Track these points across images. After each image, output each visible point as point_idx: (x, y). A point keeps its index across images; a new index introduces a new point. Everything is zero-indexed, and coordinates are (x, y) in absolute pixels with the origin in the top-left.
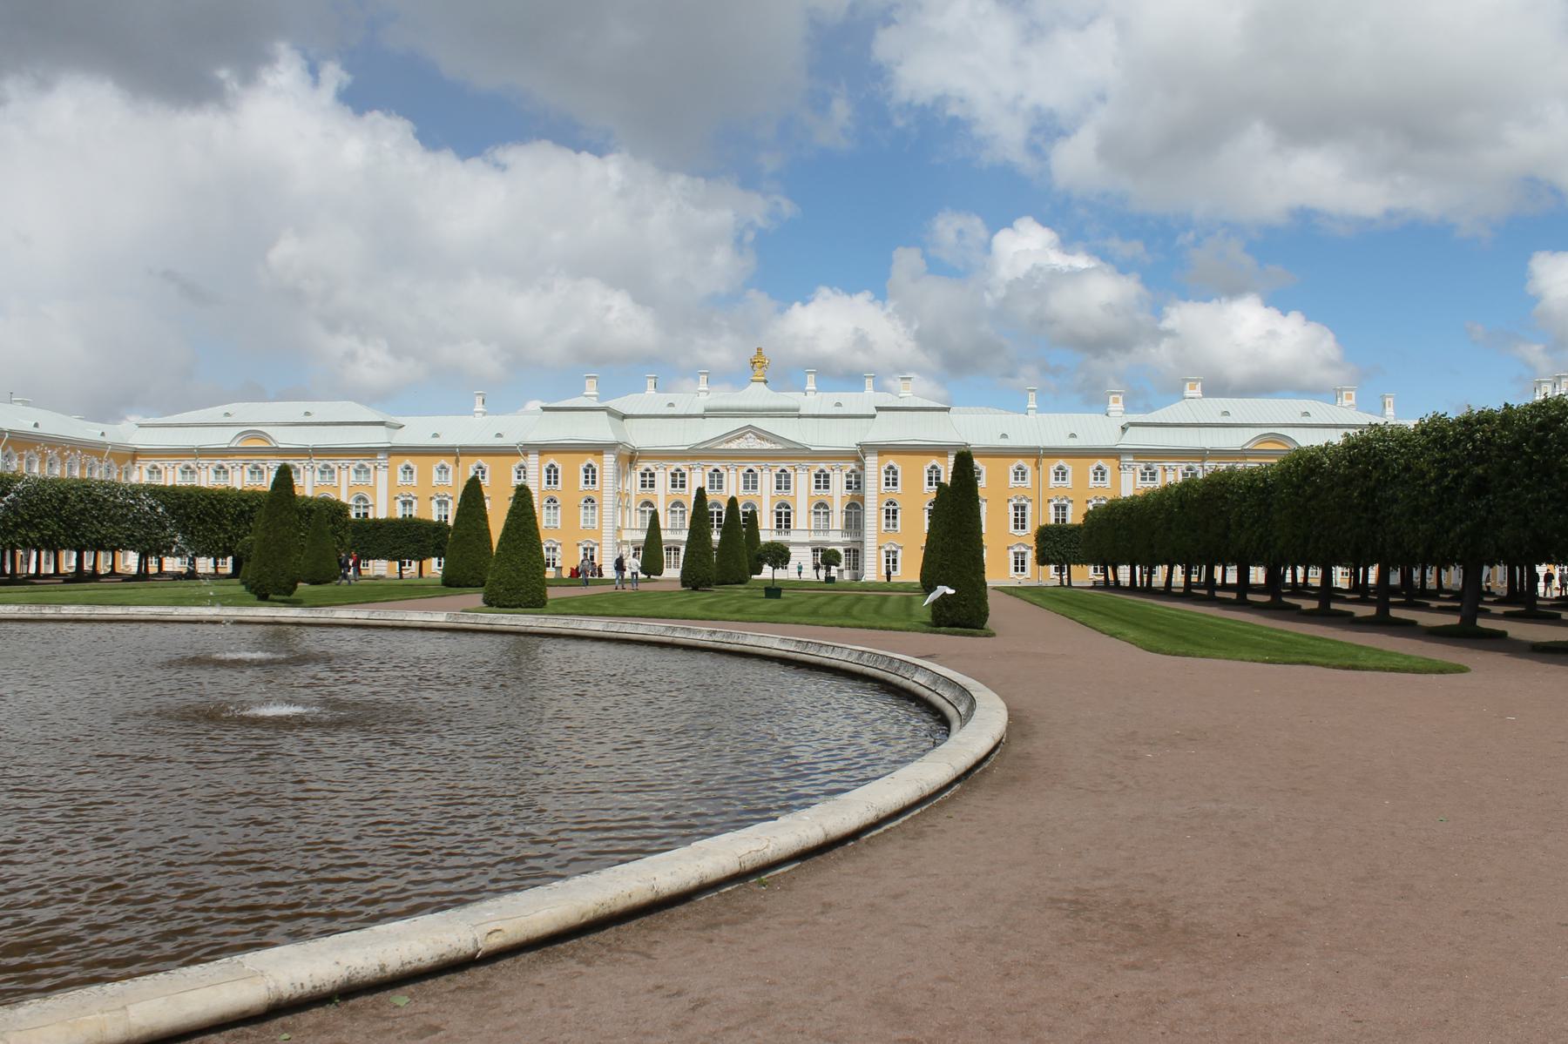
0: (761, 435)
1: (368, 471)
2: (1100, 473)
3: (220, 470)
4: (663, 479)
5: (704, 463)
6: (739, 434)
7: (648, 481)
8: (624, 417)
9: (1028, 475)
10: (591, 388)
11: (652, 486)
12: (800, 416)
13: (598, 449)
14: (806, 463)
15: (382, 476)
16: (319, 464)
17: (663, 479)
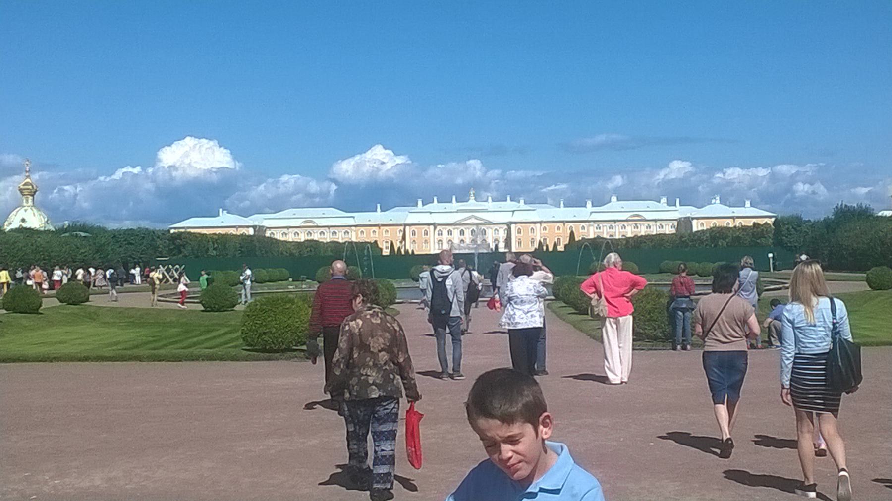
0: (476, 218)
1: (348, 233)
2: (583, 228)
3: (296, 234)
4: (445, 233)
5: (458, 227)
6: (470, 218)
7: (440, 234)
8: (431, 213)
9: (561, 229)
10: (420, 202)
11: (441, 234)
12: (488, 212)
13: (429, 225)
14: (492, 226)
15: (354, 234)
16: (332, 230)
17: (445, 233)
